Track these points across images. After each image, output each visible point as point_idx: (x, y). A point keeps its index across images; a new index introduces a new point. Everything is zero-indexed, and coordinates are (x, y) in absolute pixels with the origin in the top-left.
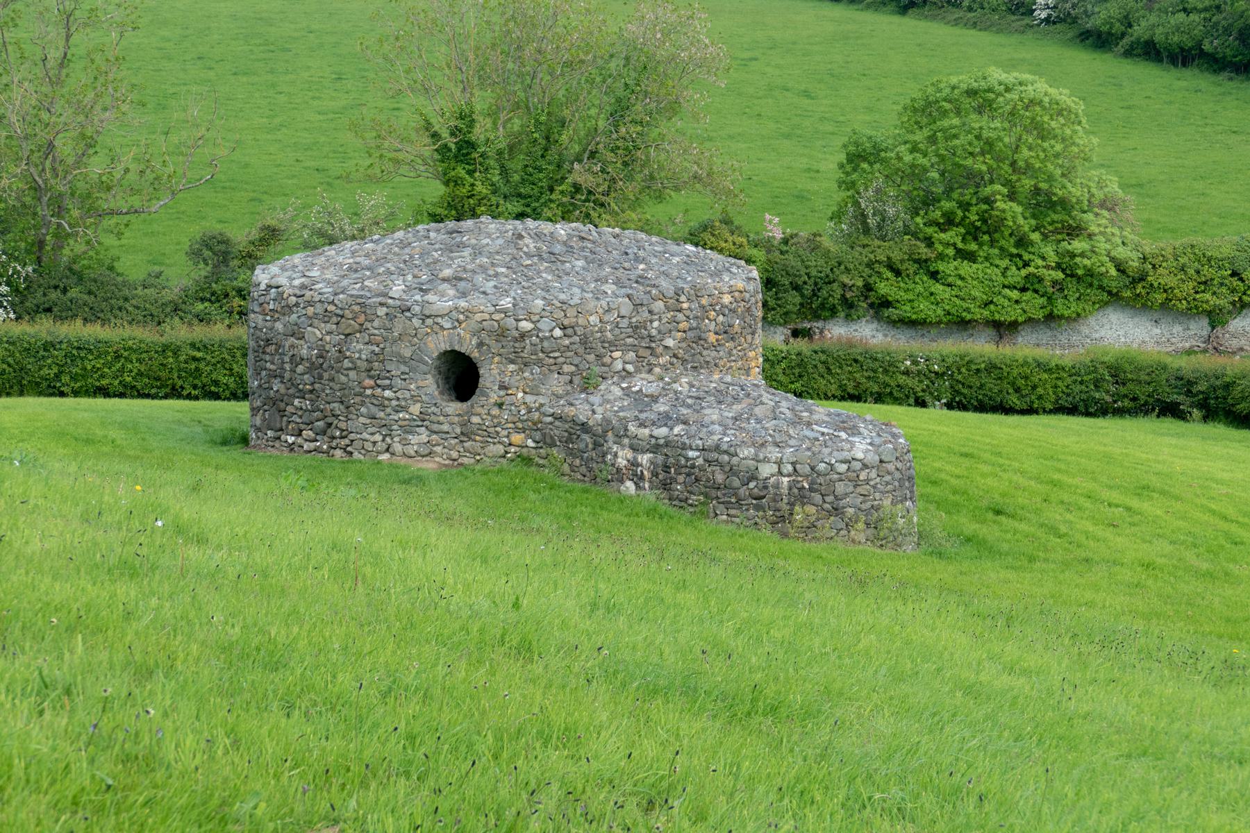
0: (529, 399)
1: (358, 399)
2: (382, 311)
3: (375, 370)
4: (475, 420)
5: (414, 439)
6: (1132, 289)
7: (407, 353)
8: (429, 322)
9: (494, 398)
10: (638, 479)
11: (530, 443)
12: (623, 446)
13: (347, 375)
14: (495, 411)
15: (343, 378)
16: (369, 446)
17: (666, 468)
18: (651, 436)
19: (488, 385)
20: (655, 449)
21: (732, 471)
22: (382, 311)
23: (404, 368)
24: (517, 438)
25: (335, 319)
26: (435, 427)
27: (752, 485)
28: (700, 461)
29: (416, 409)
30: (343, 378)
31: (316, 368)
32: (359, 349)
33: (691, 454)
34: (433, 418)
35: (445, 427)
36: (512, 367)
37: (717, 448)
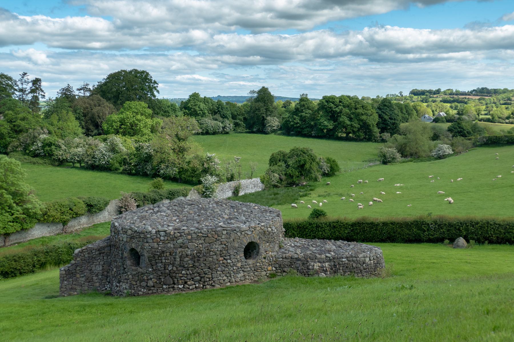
0: (273, 254)
1: (217, 266)
2: (225, 232)
3: (224, 254)
4: (258, 264)
5: (239, 276)
6: (44, 219)
7: (237, 245)
8: (243, 233)
9: (263, 256)
10: (325, 271)
11: (274, 269)
12: (315, 262)
13: (212, 258)
14: (264, 260)
15: (211, 259)
16: (222, 281)
17: (335, 266)
18: (327, 257)
19: (262, 251)
20: (330, 260)
21: (358, 262)
22: (225, 232)
23: (235, 251)
24: (270, 268)
25: (203, 238)
26: (246, 270)
27: (364, 265)
28: (347, 262)
29: (239, 265)
30: (211, 259)
31: (195, 258)
32: (217, 247)
33: (343, 260)
34: (245, 267)
35: (249, 269)
36: (268, 244)
37: (352, 256)
